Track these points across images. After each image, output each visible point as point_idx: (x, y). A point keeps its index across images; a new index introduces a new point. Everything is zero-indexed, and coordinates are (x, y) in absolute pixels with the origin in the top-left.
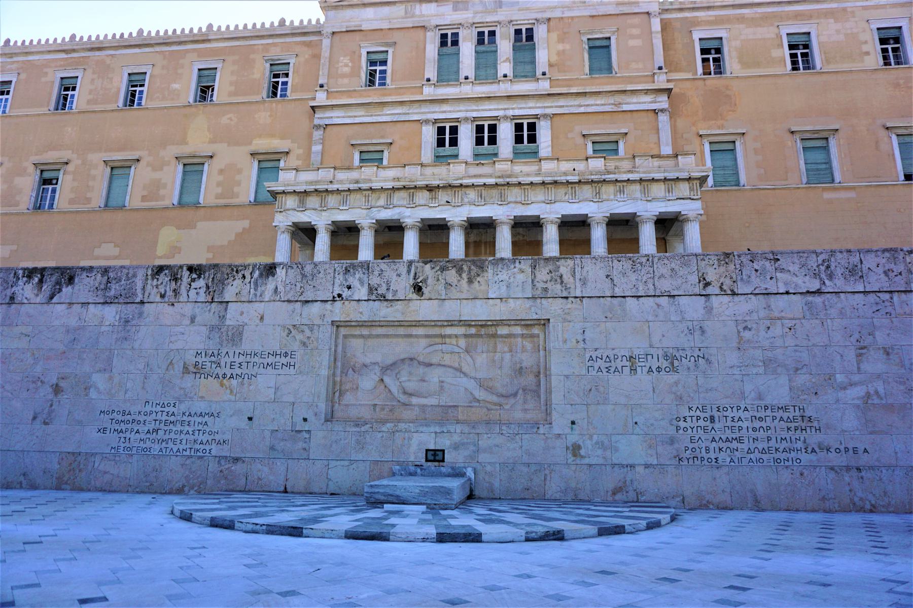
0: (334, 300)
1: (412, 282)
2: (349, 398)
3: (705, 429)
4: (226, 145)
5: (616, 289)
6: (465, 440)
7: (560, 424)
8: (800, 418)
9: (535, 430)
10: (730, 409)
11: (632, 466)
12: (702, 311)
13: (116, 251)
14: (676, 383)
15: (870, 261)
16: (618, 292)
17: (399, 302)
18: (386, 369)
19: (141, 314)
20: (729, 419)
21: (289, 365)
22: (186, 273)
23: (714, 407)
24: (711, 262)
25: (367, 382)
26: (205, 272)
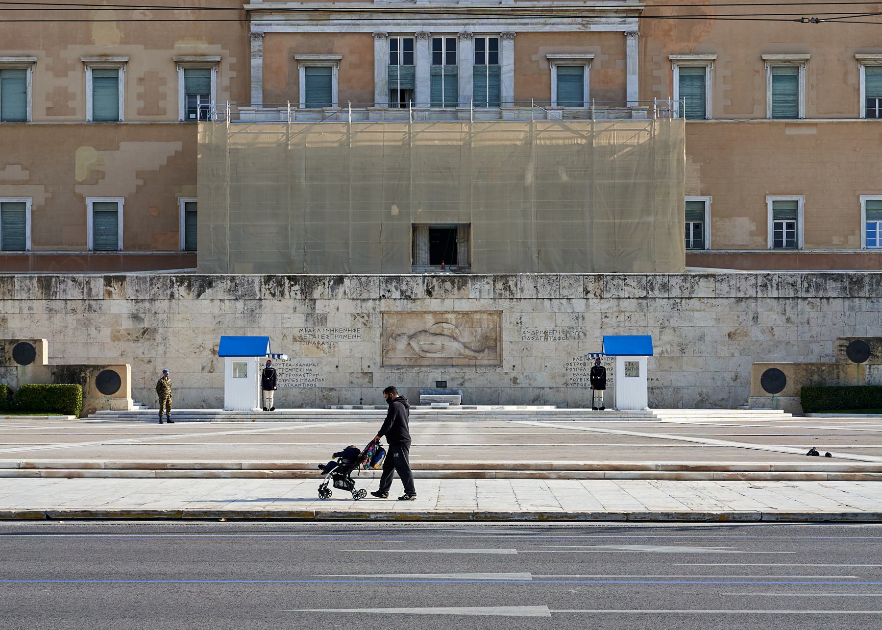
0: (380, 299)
1: (425, 288)
2: (391, 354)
3: (580, 369)
4: (142, 46)
7: (507, 367)
11: (543, 388)
12: (584, 307)
13: (25, 175)
14: (568, 346)
15: (673, 281)
16: (540, 296)
18: (411, 337)
19: (261, 306)
21: (356, 336)
22: (287, 281)
25: (401, 345)
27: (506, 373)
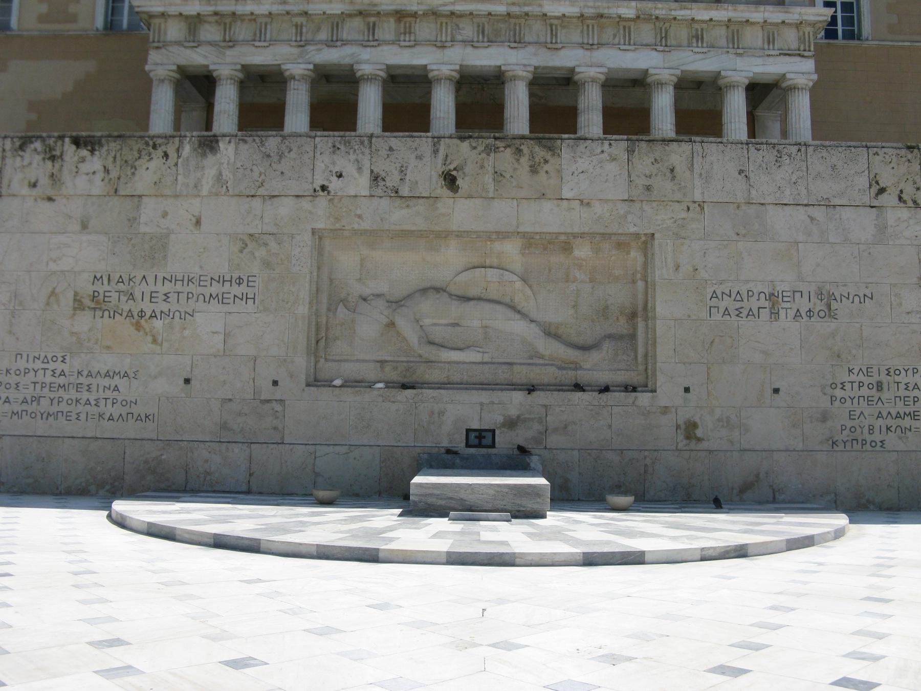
1: (440, 169)
3: (869, 400)
5: (753, 192)
6: (527, 416)
7: (667, 392)
9: (631, 401)
10: (903, 372)
17: (421, 201)
18: (397, 303)
20: (902, 386)
21: (245, 298)
23: (883, 369)
24: (888, 159)
25: (368, 326)
26: (101, 145)
27: (665, 410)
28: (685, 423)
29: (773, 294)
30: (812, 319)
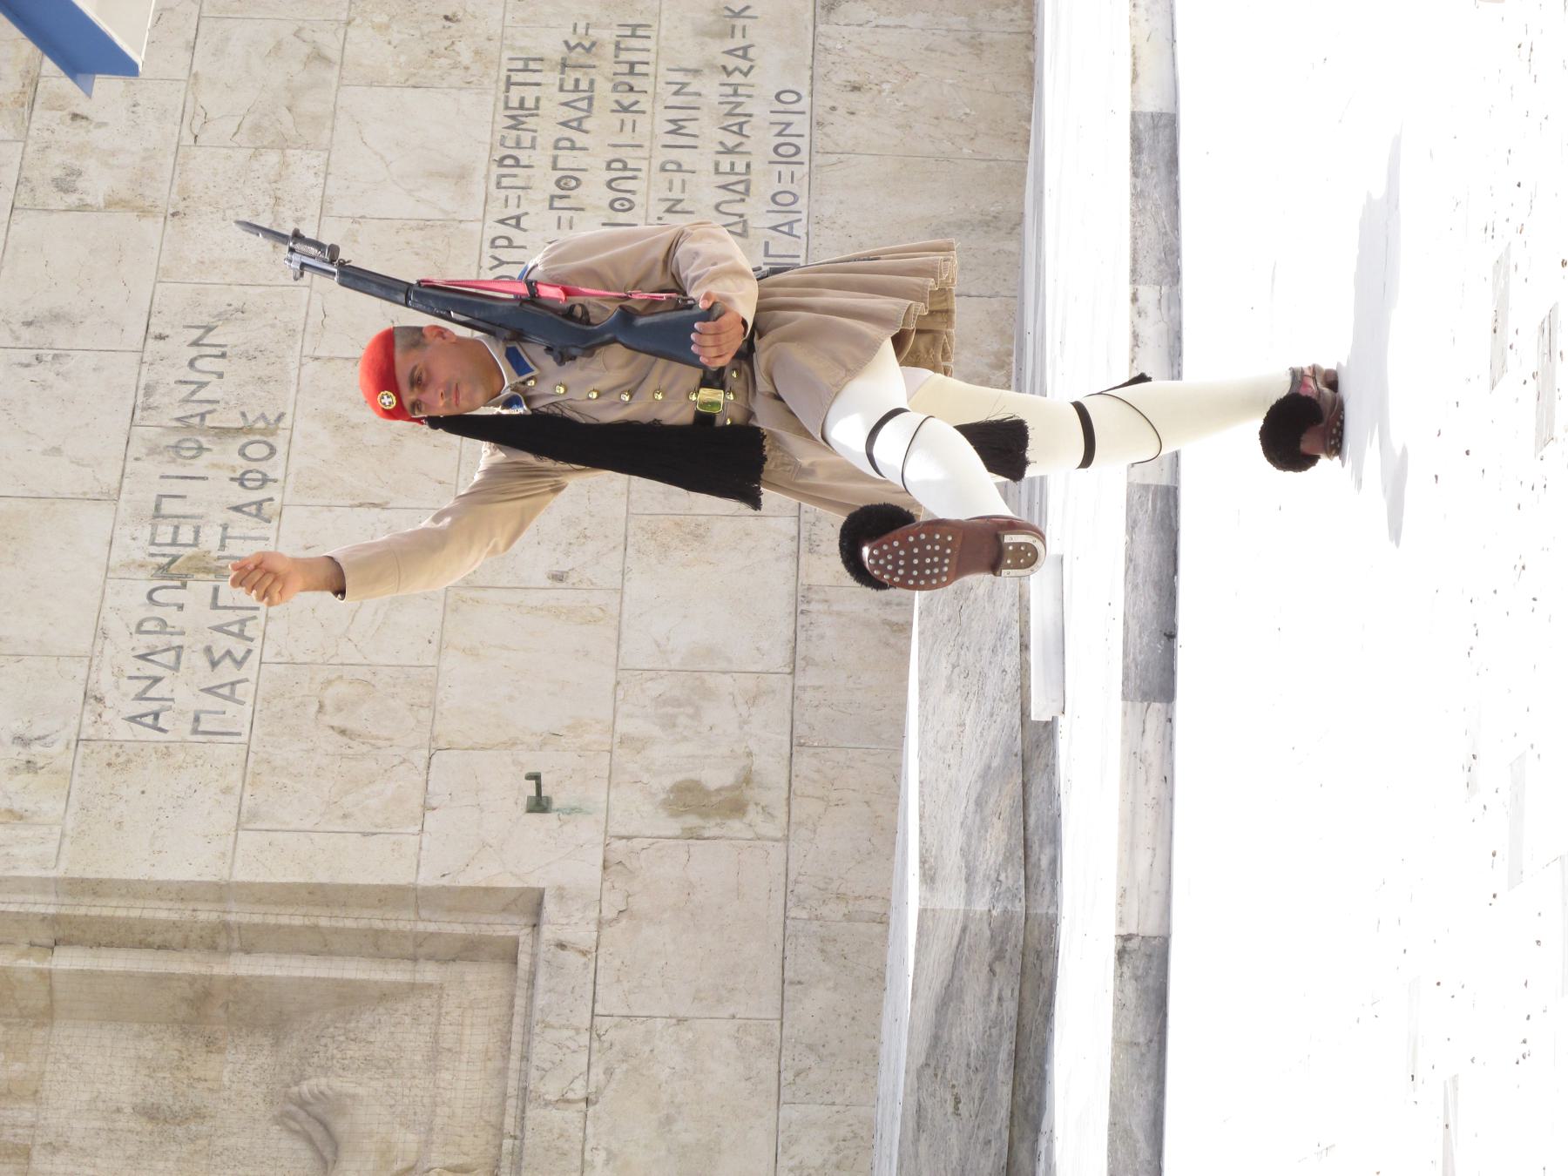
8: (572, 75)
9: (570, 957)
28: (675, 815)
29: (161, 568)
30: (277, 474)
